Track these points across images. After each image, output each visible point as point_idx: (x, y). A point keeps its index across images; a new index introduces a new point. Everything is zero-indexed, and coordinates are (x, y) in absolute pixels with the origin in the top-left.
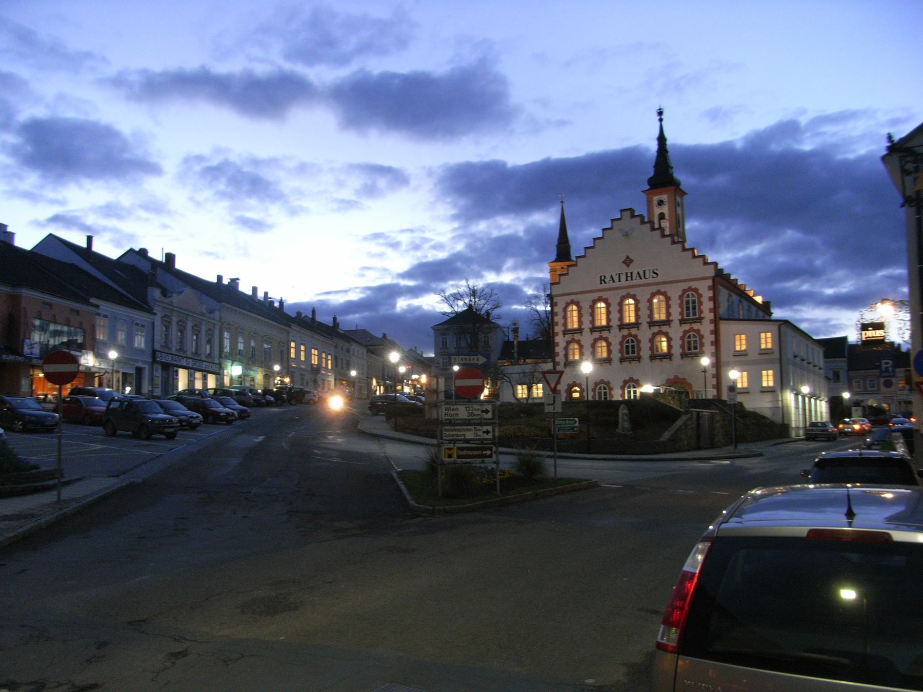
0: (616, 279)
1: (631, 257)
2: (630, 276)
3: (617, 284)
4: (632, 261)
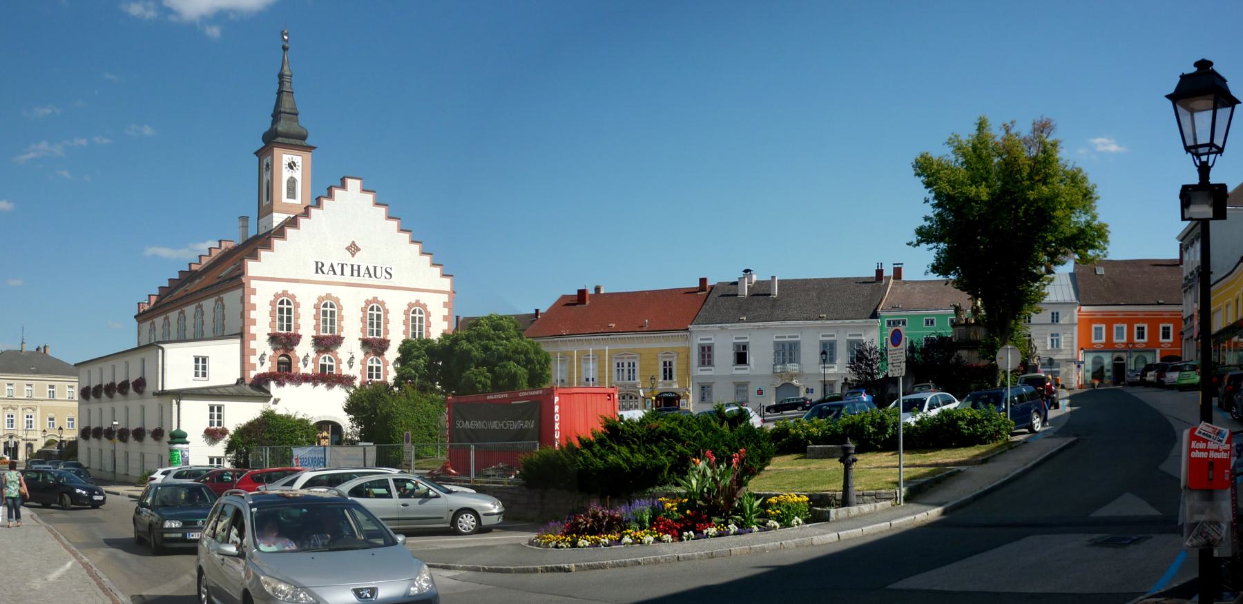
0: (338, 269)
3: (338, 278)
4: (358, 250)
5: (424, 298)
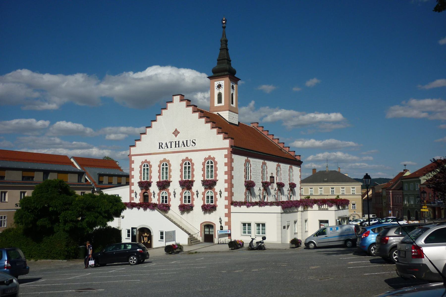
0: (169, 145)
1: (178, 130)
2: (177, 144)
3: (169, 150)
5: (212, 154)
